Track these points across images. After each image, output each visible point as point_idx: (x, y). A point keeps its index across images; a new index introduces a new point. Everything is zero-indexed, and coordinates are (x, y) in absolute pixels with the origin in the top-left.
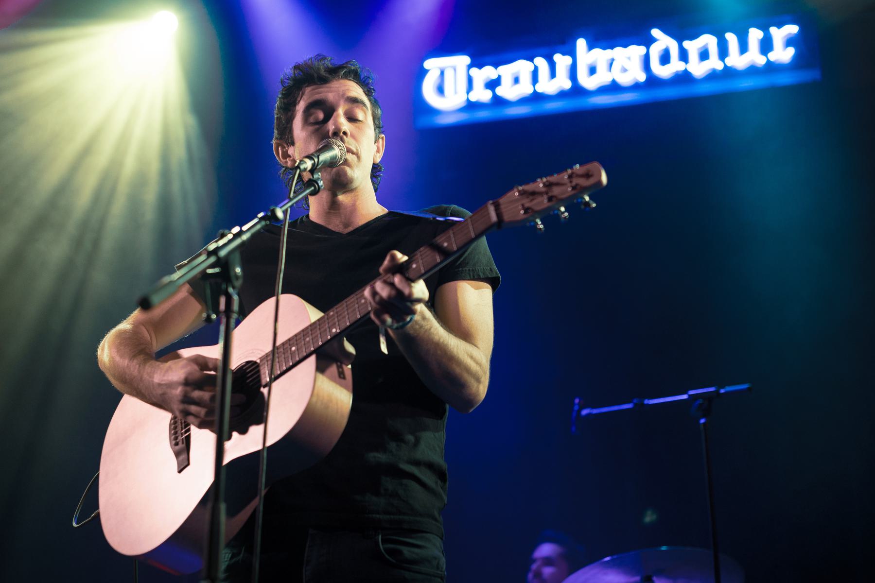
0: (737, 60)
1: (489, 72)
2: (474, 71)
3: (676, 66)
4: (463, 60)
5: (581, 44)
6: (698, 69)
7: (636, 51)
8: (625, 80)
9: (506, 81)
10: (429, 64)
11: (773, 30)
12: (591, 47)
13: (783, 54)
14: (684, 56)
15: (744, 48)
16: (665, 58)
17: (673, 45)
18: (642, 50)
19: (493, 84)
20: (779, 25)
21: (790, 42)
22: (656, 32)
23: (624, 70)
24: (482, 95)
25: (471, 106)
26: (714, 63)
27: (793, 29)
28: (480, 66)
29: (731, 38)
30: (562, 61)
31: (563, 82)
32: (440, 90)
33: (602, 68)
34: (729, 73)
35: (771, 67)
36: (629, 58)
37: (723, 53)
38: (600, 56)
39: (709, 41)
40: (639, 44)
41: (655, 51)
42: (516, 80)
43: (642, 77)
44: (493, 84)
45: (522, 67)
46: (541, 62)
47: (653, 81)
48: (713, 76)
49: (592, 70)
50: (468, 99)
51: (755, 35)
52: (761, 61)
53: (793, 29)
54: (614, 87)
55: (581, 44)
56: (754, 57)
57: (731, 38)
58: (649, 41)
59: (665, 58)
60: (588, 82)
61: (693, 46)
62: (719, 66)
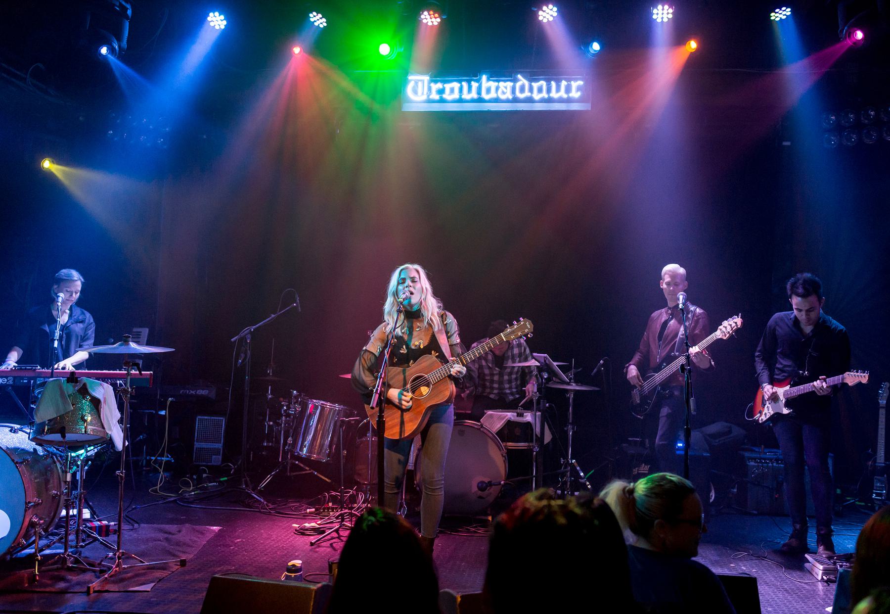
0: (554, 95)
1: (439, 86)
2: (432, 85)
3: (527, 94)
4: (426, 78)
5: (484, 77)
6: (536, 96)
7: (509, 84)
8: (503, 97)
9: (447, 91)
10: (410, 78)
11: (572, 82)
12: (488, 80)
13: (575, 94)
14: (531, 90)
15: (558, 90)
16: (522, 90)
17: (526, 83)
18: (512, 84)
19: (441, 92)
20: (576, 80)
21: (579, 89)
22: (519, 76)
23: (504, 93)
24: (435, 96)
25: (430, 101)
26: (544, 95)
27: (581, 83)
28: (436, 82)
29: (553, 84)
30: (475, 85)
31: (474, 95)
32: (415, 92)
33: (493, 90)
34: (550, 100)
35: (569, 101)
36: (506, 88)
37: (549, 90)
38: (493, 85)
39: (543, 83)
40: (511, 81)
41: (518, 85)
42: (452, 90)
43: (511, 97)
44: (441, 92)
45: (456, 85)
46: (465, 84)
47: (515, 100)
48: (543, 101)
49: (488, 91)
50: (428, 96)
51: (564, 83)
52: (565, 96)
53: (581, 83)
54: (497, 100)
55: (484, 77)
56: (562, 94)
57: (553, 84)
58: (515, 80)
59: (522, 90)
60: (485, 96)
61: (535, 85)
62: (546, 96)
